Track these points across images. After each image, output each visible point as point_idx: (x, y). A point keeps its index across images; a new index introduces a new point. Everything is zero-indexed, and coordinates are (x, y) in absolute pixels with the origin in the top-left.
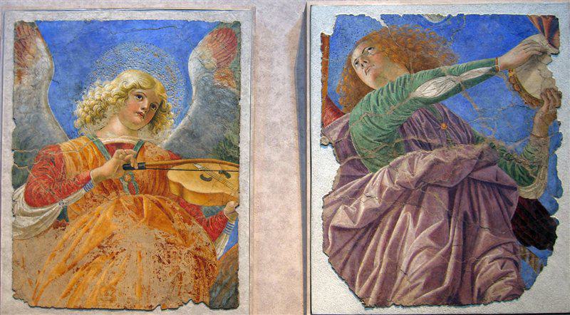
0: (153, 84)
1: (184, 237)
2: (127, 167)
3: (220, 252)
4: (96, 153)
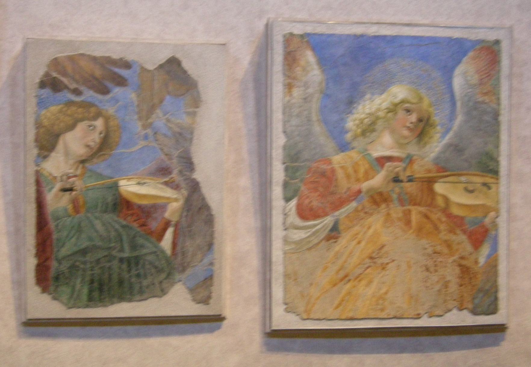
0: (421, 99)
2: (396, 180)
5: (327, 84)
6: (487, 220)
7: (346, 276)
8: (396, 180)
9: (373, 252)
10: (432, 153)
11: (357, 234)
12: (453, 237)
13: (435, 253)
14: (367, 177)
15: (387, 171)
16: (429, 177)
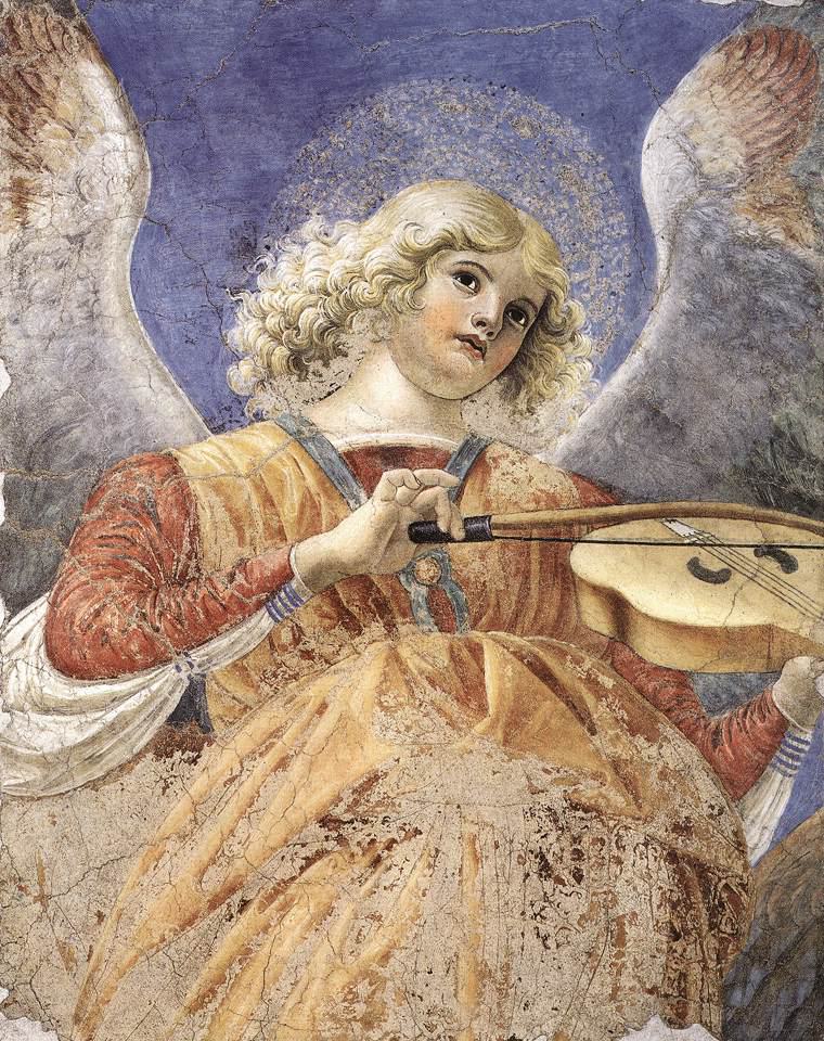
1: (629, 785)
2: (424, 532)
3: (759, 839)
4: (311, 481)
8: (424, 532)
14: (311, 524)
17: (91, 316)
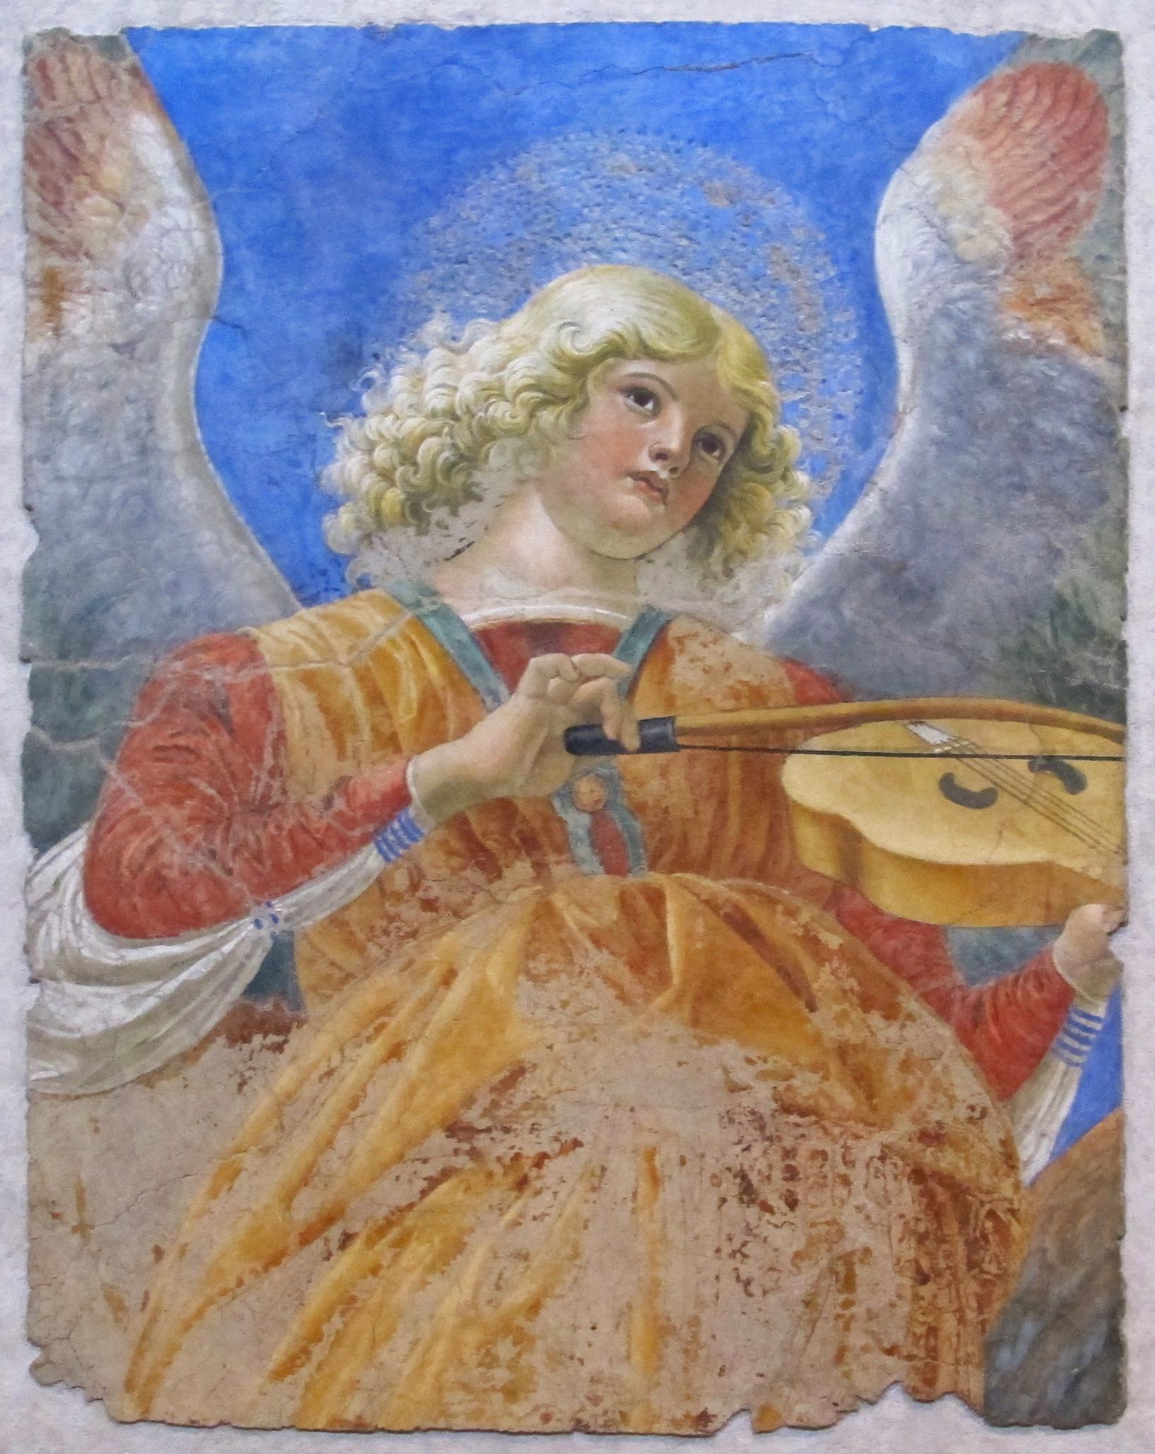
0: (707, 334)
4: (433, 670)
5: (230, 269)
6: (1063, 950)
7: (329, 1219)
9: (469, 1101)
10: (768, 602)
11: (387, 1010)
12: (887, 1032)
13: (787, 1109)
15: (539, 696)
16: (752, 729)
17: (144, 451)
